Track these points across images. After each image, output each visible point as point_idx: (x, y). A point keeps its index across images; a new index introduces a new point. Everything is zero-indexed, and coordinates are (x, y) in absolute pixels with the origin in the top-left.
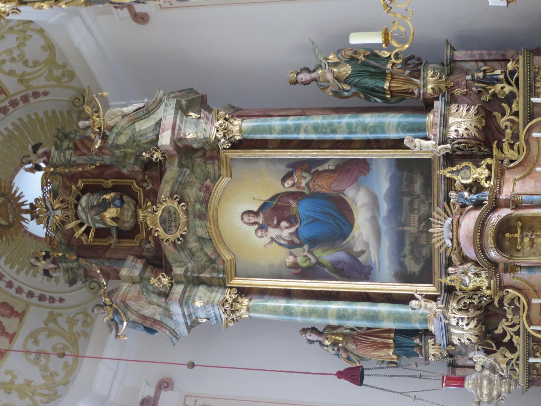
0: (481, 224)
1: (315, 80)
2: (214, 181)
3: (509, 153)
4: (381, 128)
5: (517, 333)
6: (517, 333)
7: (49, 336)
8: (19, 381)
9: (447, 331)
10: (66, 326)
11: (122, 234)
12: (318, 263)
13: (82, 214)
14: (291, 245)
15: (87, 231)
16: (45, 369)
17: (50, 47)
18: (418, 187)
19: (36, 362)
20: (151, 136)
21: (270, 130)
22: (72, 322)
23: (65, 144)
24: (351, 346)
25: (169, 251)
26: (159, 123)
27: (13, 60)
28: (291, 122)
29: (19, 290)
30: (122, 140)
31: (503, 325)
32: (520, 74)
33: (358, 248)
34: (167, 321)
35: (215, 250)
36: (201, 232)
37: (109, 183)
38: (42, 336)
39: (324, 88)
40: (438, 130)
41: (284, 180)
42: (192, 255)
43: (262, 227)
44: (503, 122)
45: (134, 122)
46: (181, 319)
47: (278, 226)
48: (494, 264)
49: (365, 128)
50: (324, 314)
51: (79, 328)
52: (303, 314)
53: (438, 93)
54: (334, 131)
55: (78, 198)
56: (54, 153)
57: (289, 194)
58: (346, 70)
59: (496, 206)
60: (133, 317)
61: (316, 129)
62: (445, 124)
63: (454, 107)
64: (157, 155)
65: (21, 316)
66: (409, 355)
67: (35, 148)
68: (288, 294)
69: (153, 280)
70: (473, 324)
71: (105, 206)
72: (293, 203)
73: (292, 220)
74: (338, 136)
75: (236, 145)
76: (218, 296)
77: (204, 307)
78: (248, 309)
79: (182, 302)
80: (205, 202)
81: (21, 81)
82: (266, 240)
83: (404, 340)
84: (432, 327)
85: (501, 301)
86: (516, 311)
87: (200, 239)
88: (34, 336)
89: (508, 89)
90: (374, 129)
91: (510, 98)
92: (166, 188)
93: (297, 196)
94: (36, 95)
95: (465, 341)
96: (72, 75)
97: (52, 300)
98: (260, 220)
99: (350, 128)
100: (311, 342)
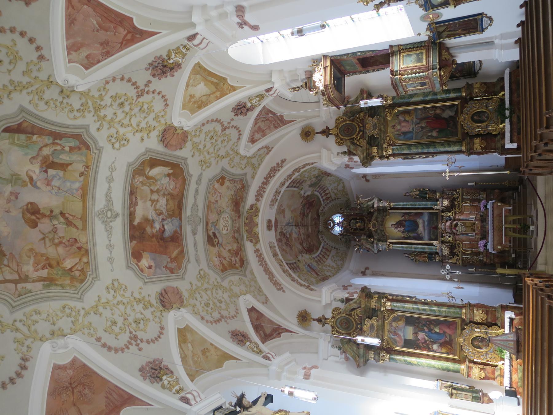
0: (451, 223)
1: (410, 195)
2: (385, 217)
3: (457, 210)
4: (427, 205)
5: (459, 252)
6: (459, 252)
7: (337, 257)
8: (331, 265)
9: (442, 251)
10: (341, 255)
11: (361, 230)
12: (410, 236)
13: (351, 224)
14: (403, 232)
15: (352, 229)
16: (336, 264)
17: (344, 187)
18: (434, 219)
19: (334, 262)
20: (371, 206)
21: (400, 205)
22: (342, 254)
23: (348, 209)
24: (417, 258)
25: (373, 233)
26: (374, 203)
27: (335, 189)
28: (405, 203)
29: (329, 246)
30: (365, 206)
31: (456, 250)
32: (460, 193)
33: (420, 233)
34: (372, 249)
35: (384, 233)
36: (381, 229)
37: (358, 218)
38: (335, 257)
39: (412, 197)
40: (441, 205)
41: (402, 217)
42: (378, 234)
43: (396, 228)
44: (456, 203)
45: (368, 202)
46: (376, 248)
47: (400, 227)
48: (454, 233)
49: (423, 205)
50: (411, 248)
51: (344, 256)
52: (406, 247)
53: (440, 197)
54: (415, 205)
55: (351, 221)
56: (345, 210)
57: (403, 220)
58: (418, 193)
59: (454, 220)
60: (364, 247)
61: (411, 205)
62: (442, 204)
63: (444, 200)
64: (372, 210)
65: (330, 251)
66: (431, 260)
67: (341, 209)
68: (402, 243)
69: (369, 239)
70: (448, 249)
71: (357, 223)
72: (404, 222)
73: (404, 226)
74: (416, 207)
75: (391, 209)
76: (385, 243)
77: (382, 246)
78: (392, 247)
79: (377, 244)
80: (383, 222)
81: (335, 195)
82: (397, 231)
83: (430, 256)
84: (438, 251)
85: (455, 244)
86: (459, 247)
87: (381, 231)
88: (333, 256)
89: (457, 196)
90: (425, 205)
91: (458, 198)
92: (374, 218)
93: (405, 221)
94: (338, 199)
95: (446, 254)
96: (347, 194)
97: (337, 249)
98: (396, 226)
99: (419, 205)
100: (406, 256)
